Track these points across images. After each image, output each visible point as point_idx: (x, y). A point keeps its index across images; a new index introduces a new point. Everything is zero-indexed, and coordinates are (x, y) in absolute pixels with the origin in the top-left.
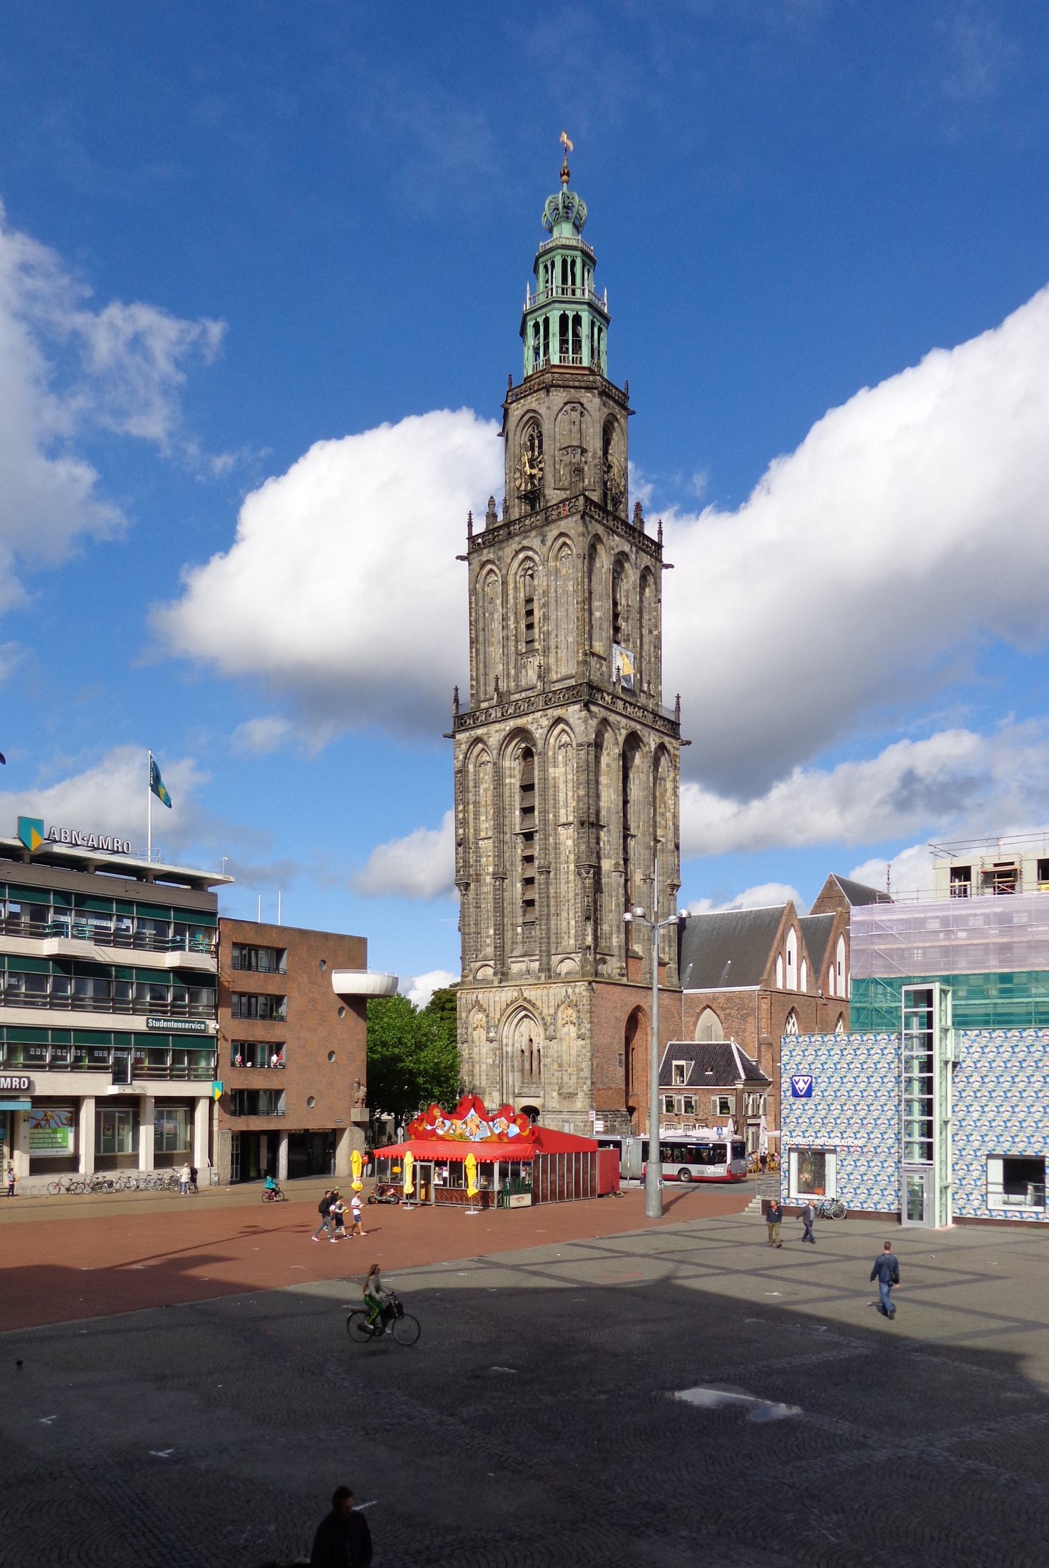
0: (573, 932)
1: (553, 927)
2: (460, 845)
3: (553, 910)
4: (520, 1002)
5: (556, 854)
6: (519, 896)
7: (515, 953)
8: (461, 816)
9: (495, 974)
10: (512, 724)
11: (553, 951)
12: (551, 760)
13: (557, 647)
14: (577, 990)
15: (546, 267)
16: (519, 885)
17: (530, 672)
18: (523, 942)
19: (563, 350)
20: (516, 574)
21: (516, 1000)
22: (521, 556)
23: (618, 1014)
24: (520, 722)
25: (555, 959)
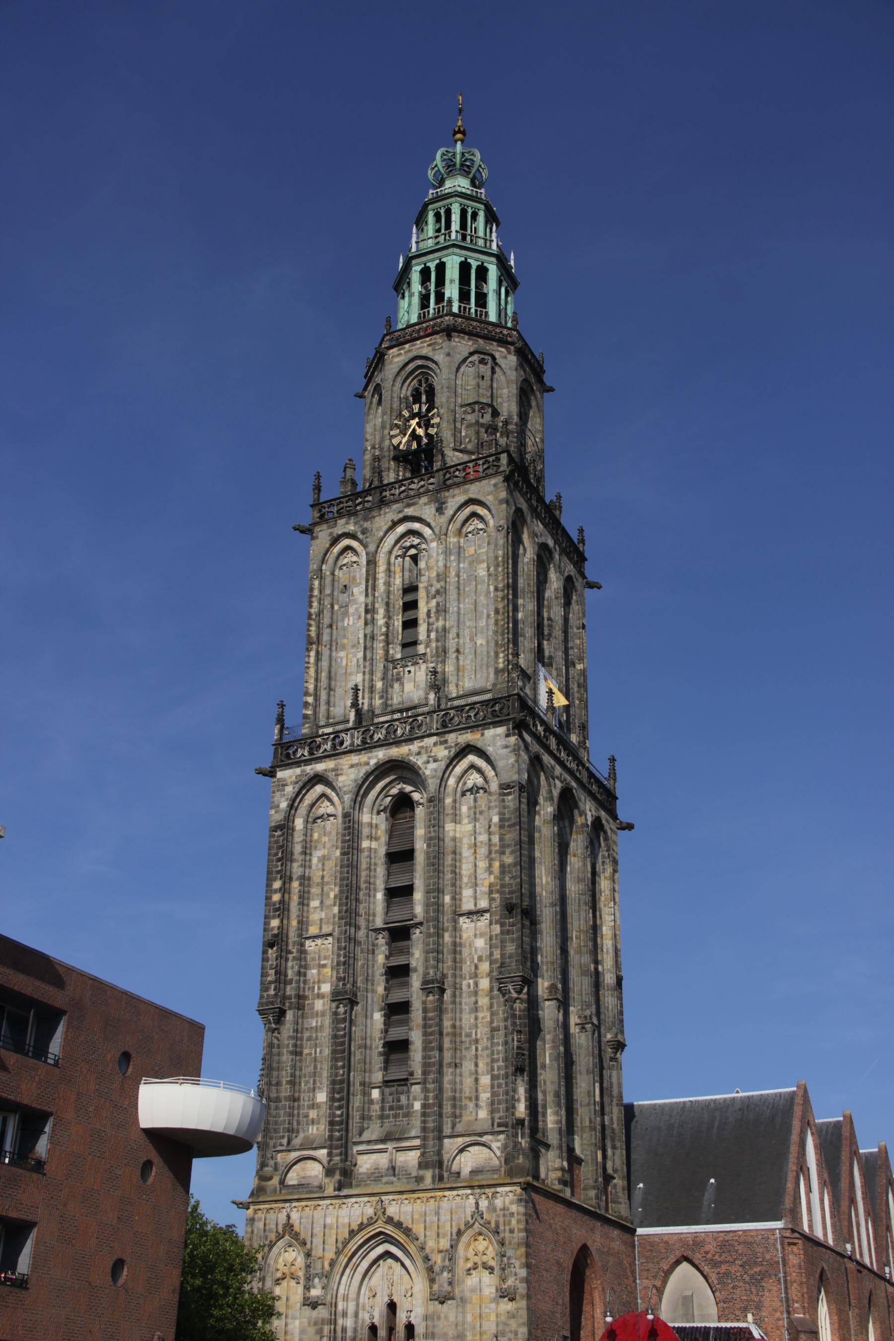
0: (485, 1096)
1: (447, 1086)
2: (271, 945)
3: (447, 1056)
5: (455, 961)
6: (377, 1034)
7: (366, 1136)
8: (276, 897)
9: (329, 1172)
10: (381, 755)
11: (447, 1130)
12: (449, 811)
13: (458, 651)
14: (499, 1202)
15: (438, 216)
16: (378, 1017)
17: (409, 687)
18: (382, 1117)
19: (464, 296)
20: (390, 552)
21: (371, 1222)
22: (401, 529)
24: (395, 752)
25: (450, 1145)
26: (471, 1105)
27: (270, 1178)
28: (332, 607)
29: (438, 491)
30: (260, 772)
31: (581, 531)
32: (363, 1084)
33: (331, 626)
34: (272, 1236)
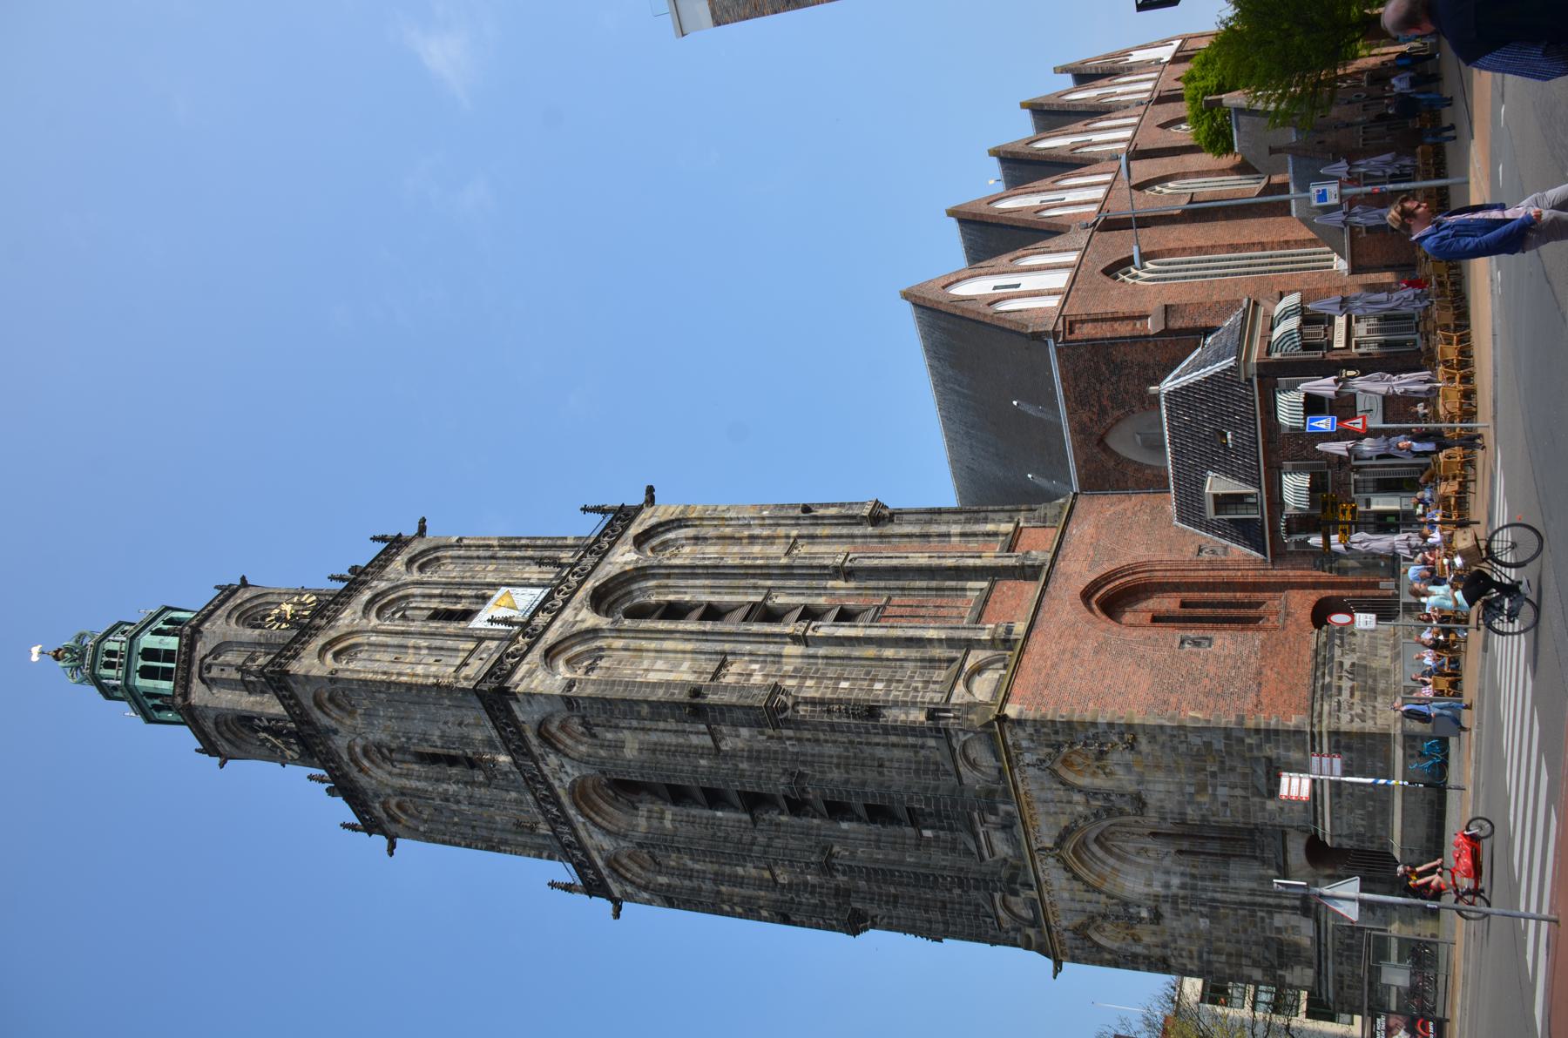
4: (1068, 853)
6: (864, 827)
19: (166, 675)
20: (390, 773)
21: (1060, 859)
22: (366, 763)
23: (1089, 645)
24: (565, 800)
26: (923, 752)
27: (1028, 937)
28: (456, 824)
29: (318, 731)
30: (617, 915)
31: (374, 539)
32: (918, 846)
33: (473, 828)
34: (1088, 944)
